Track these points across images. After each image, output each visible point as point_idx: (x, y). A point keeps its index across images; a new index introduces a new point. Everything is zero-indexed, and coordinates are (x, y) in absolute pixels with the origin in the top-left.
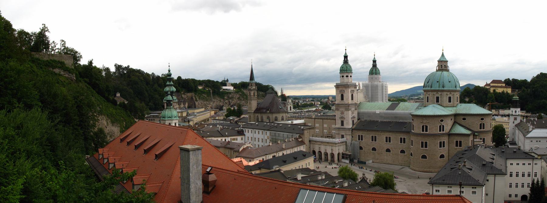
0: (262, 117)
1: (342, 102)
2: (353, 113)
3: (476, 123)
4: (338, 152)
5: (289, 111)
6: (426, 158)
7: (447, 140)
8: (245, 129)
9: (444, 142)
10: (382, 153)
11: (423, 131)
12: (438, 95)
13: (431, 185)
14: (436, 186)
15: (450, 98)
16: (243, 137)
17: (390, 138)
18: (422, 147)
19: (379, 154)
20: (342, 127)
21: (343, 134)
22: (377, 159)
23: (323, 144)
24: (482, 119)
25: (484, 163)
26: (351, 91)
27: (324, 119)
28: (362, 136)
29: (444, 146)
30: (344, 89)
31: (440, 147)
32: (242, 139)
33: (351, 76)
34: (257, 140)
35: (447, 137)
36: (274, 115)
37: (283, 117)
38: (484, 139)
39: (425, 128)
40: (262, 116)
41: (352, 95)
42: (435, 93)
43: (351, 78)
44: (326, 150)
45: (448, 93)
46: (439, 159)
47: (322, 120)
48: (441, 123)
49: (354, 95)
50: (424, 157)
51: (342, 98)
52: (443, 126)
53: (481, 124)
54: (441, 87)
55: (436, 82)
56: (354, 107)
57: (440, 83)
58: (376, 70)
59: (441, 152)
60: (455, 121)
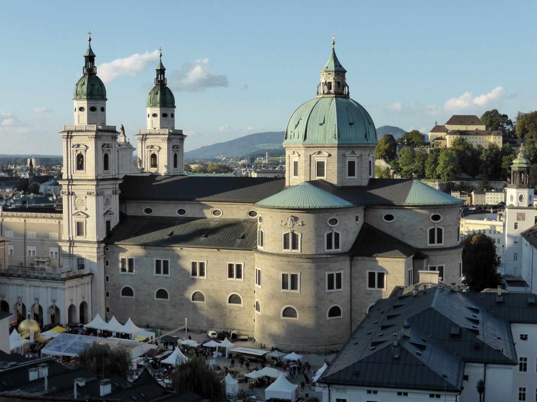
2: (107, 202)
3: (421, 227)
7: (348, 270)
9: (339, 276)
10: (182, 304)
11: (286, 246)
13: (326, 385)
14: (337, 389)
15: (352, 165)
19: (174, 306)
22: (171, 319)
23: (28, 284)
24: (436, 218)
25: (454, 331)
26: (103, 146)
27: (28, 217)
29: (339, 286)
31: (331, 287)
33: (103, 109)
35: (348, 263)
38: (441, 269)
41: (106, 157)
43: (103, 113)
44: (37, 299)
45: (348, 153)
46: (328, 318)
47: (22, 220)
48: (331, 228)
49: (109, 156)
51: (80, 166)
52: (337, 235)
53: (434, 229)
54: (330, 137)
56: (111, 186)
57: (328, 129)
58: (165, 94)
59: (331, 301)
60: (365, 223)
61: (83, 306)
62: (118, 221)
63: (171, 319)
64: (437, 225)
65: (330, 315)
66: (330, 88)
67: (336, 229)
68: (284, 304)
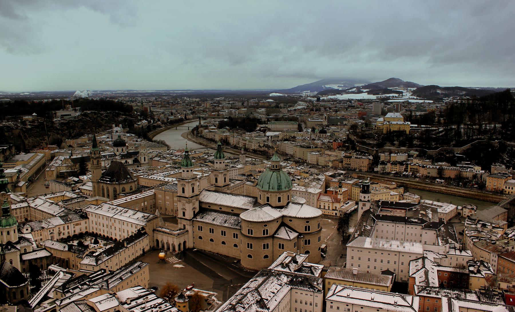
0: (108, 188)
1: (183, 195)
4: (179, 243)
5: (142, 163)
6: (252, 258)
8: (88, 212)
9: (268, 245)
11: (249, 233)
12: (269, 195)
16: (87, 220)
17: (225, 232)
18: (248, 247)
19: (216, 245)
20: (184, 217)
21: (185, 224)
22: (215, 249)
24: (308, 222)
28: (201, 227)
29: (268, 248)
30: (185, 183)
31: (264, 248)
32: (86, 223)
34: (102, 225)
36: (121, 187)
37: (131, 186)
39: (250, 231)
40: (108, 187)
42: (265, 193)
44: (168, 241)
45: (278, 194)
46: (263, 259)
50: (250, 256)
52: (267, 230)
55: (267, 183)
61: (185, 243)
62: (198, 210)
63: (215, 249)
64: (308, 224)
65: (264, 258)
66: (273, 167)
67: (266, 228)
68: (248, 253)
